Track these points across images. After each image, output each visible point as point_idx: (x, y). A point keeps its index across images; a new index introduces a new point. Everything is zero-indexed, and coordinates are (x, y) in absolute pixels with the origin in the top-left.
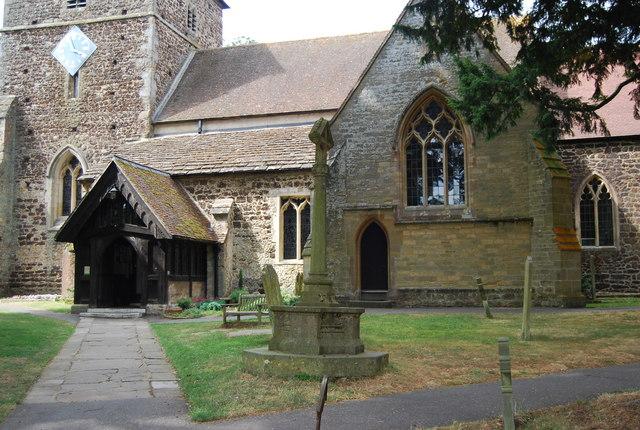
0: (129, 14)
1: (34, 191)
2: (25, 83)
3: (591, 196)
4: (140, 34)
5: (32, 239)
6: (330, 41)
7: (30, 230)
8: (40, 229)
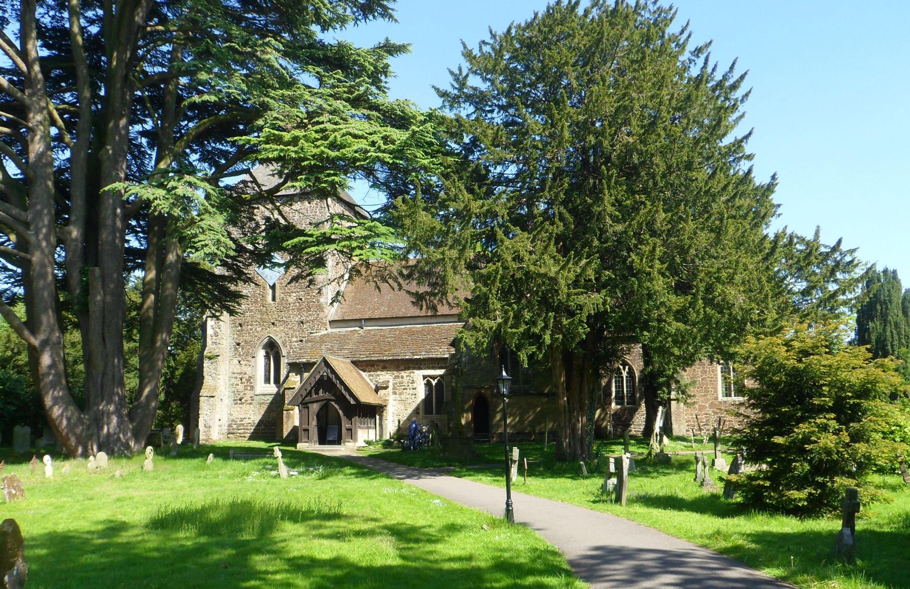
8: (249, 394)
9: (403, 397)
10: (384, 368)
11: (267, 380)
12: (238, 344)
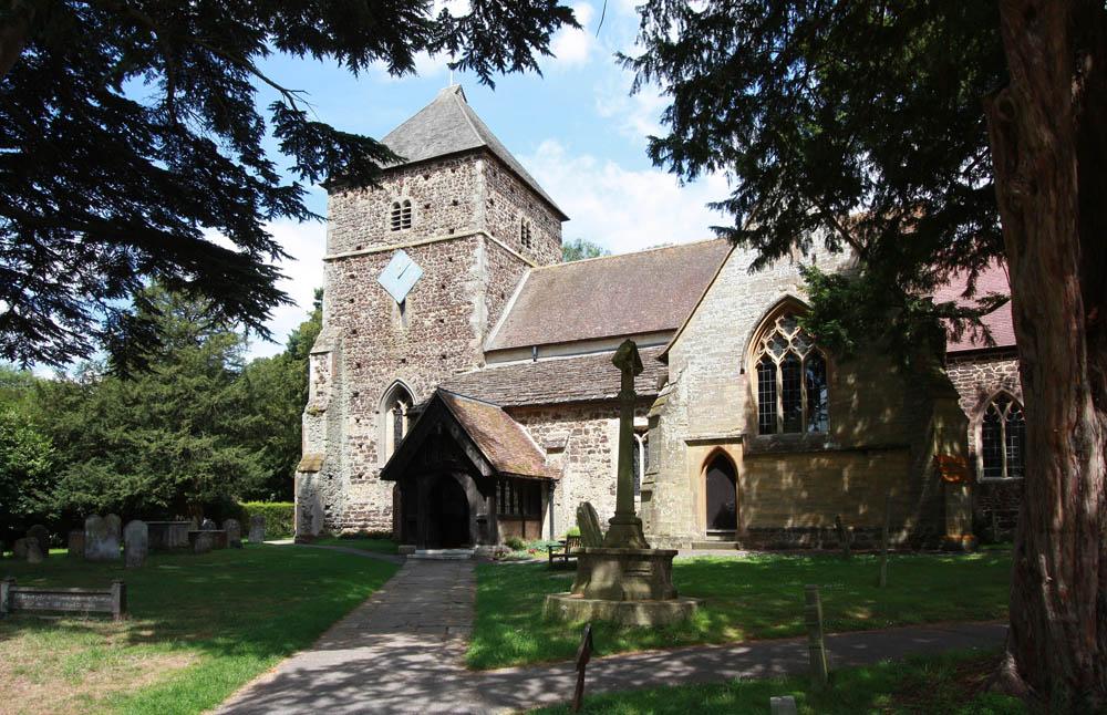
0: (457, 234)
2: (350, 314)
3: (997, 417)
6: (680, 250)
7: (361, 468)
9: (588, 466)
10: (557, 417)
12: (356, 394)
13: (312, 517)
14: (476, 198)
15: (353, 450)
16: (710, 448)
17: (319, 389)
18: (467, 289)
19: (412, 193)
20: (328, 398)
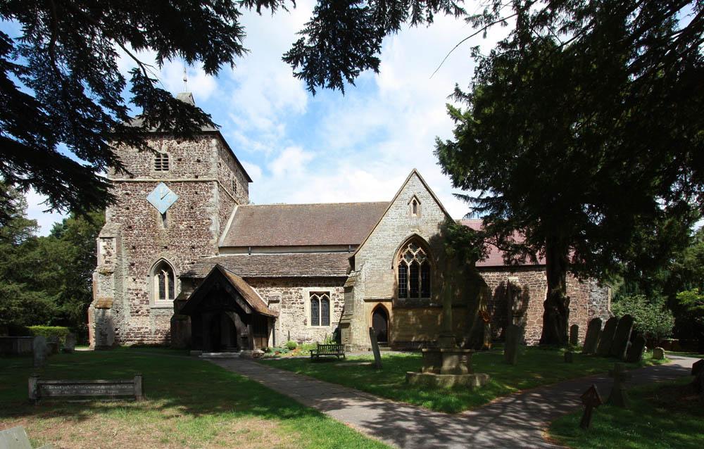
0: (200, 179)
1: (138, 284)
4: (208, 192)
5: (140, 313)
7: (138, 307)
8: (145, 307)
9: (292, 310)
10: (274, 285)
11: (162, 296)
12: (133, 264)
13: (107, 335)
14: (212, 160)
15: (131, 297)
16: (376, 304)
17: (107, 259)
18: (208, 211)
19: (169, 150)
20: (114, 265)
